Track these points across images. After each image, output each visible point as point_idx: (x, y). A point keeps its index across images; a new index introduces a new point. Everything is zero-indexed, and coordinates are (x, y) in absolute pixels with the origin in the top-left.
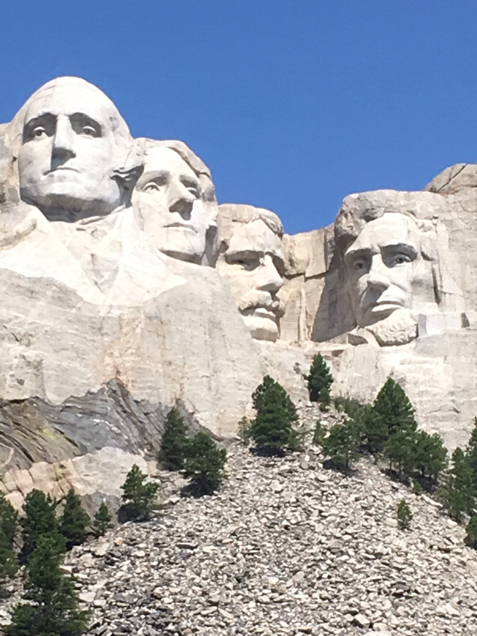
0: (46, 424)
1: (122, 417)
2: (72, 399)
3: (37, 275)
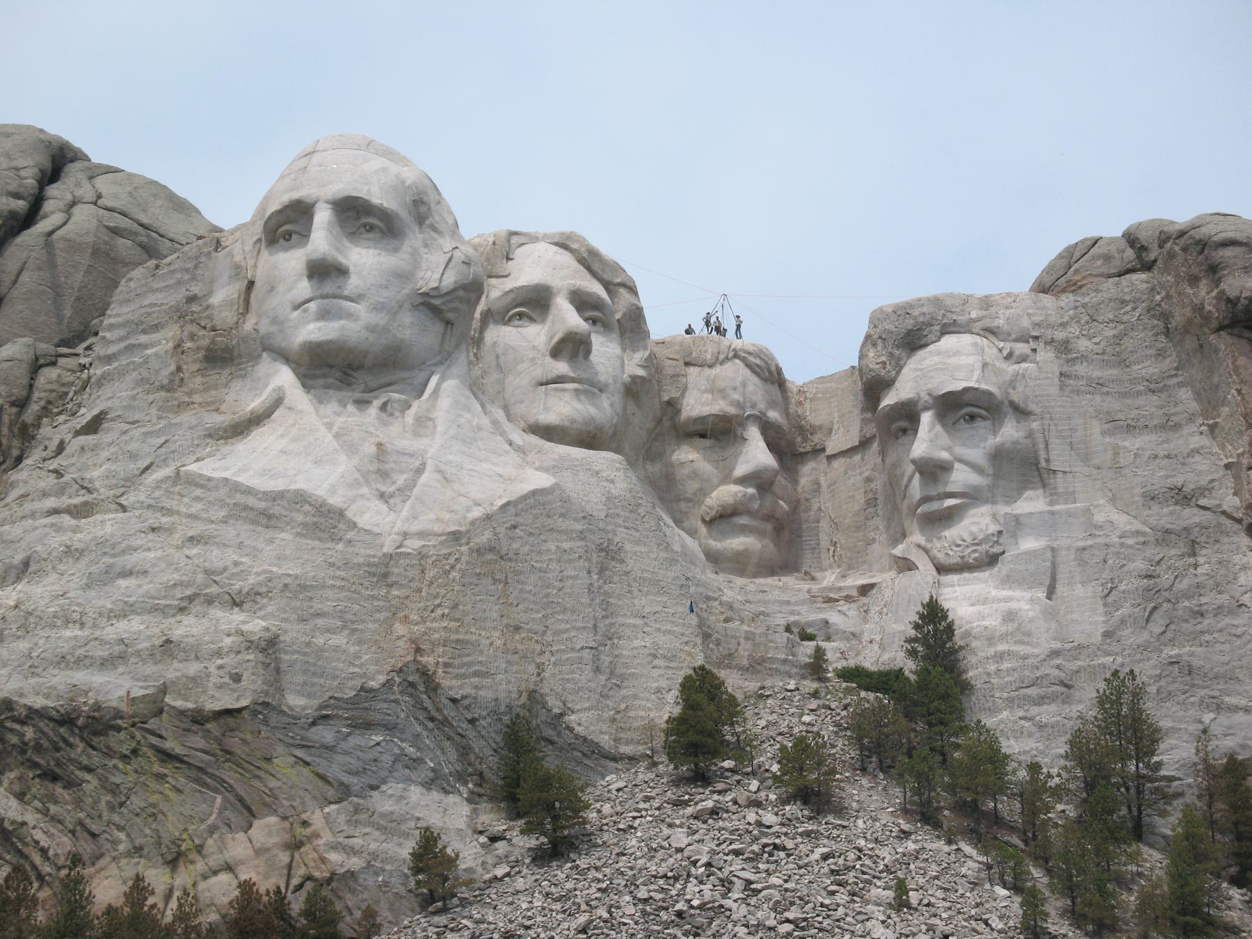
0: (280, 749)
1: (426, 728)
2: (332, 701)
3: (279, 485)
